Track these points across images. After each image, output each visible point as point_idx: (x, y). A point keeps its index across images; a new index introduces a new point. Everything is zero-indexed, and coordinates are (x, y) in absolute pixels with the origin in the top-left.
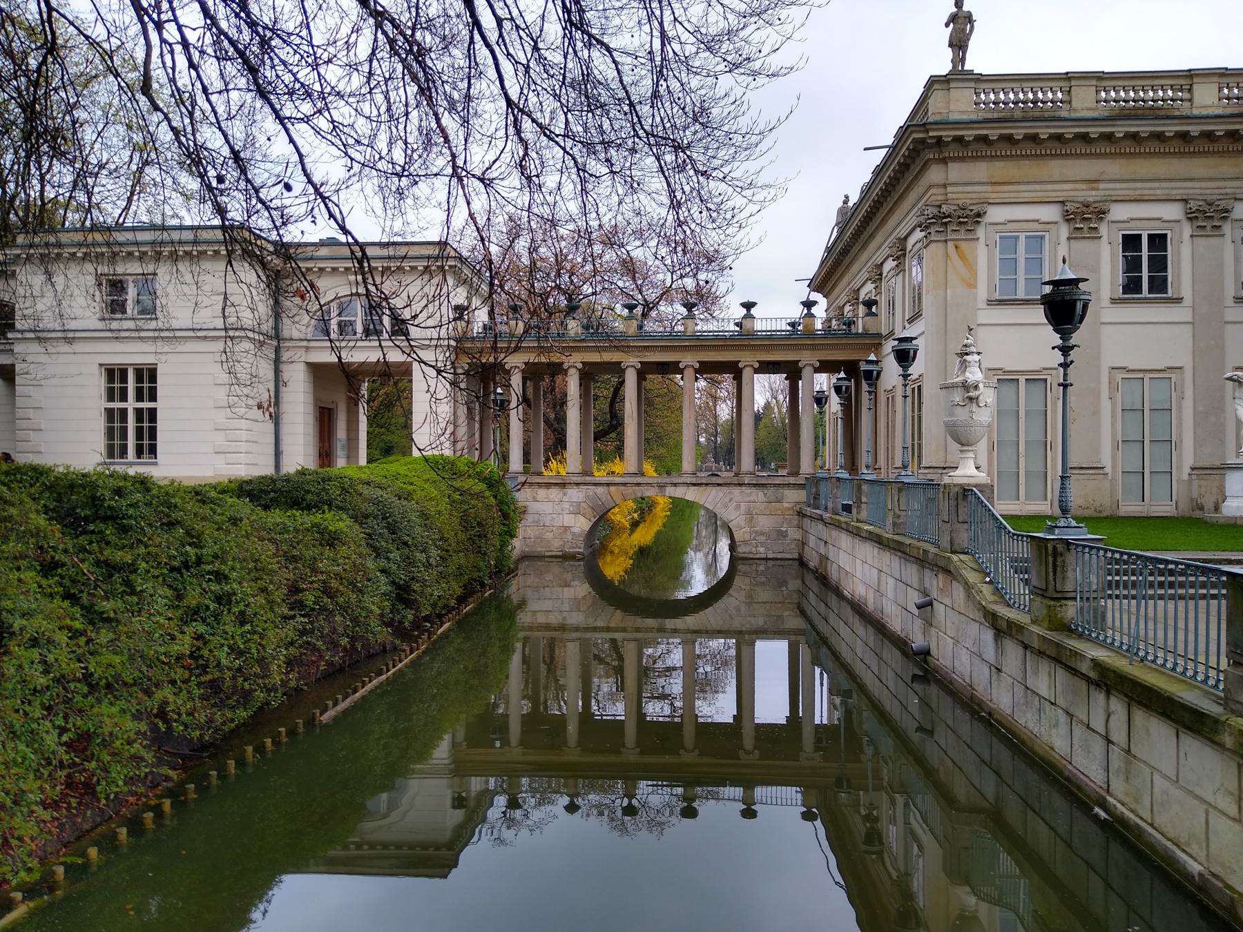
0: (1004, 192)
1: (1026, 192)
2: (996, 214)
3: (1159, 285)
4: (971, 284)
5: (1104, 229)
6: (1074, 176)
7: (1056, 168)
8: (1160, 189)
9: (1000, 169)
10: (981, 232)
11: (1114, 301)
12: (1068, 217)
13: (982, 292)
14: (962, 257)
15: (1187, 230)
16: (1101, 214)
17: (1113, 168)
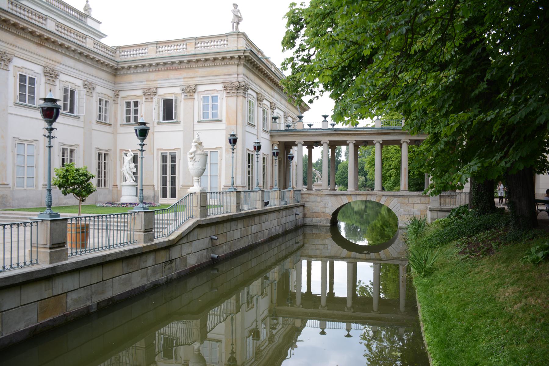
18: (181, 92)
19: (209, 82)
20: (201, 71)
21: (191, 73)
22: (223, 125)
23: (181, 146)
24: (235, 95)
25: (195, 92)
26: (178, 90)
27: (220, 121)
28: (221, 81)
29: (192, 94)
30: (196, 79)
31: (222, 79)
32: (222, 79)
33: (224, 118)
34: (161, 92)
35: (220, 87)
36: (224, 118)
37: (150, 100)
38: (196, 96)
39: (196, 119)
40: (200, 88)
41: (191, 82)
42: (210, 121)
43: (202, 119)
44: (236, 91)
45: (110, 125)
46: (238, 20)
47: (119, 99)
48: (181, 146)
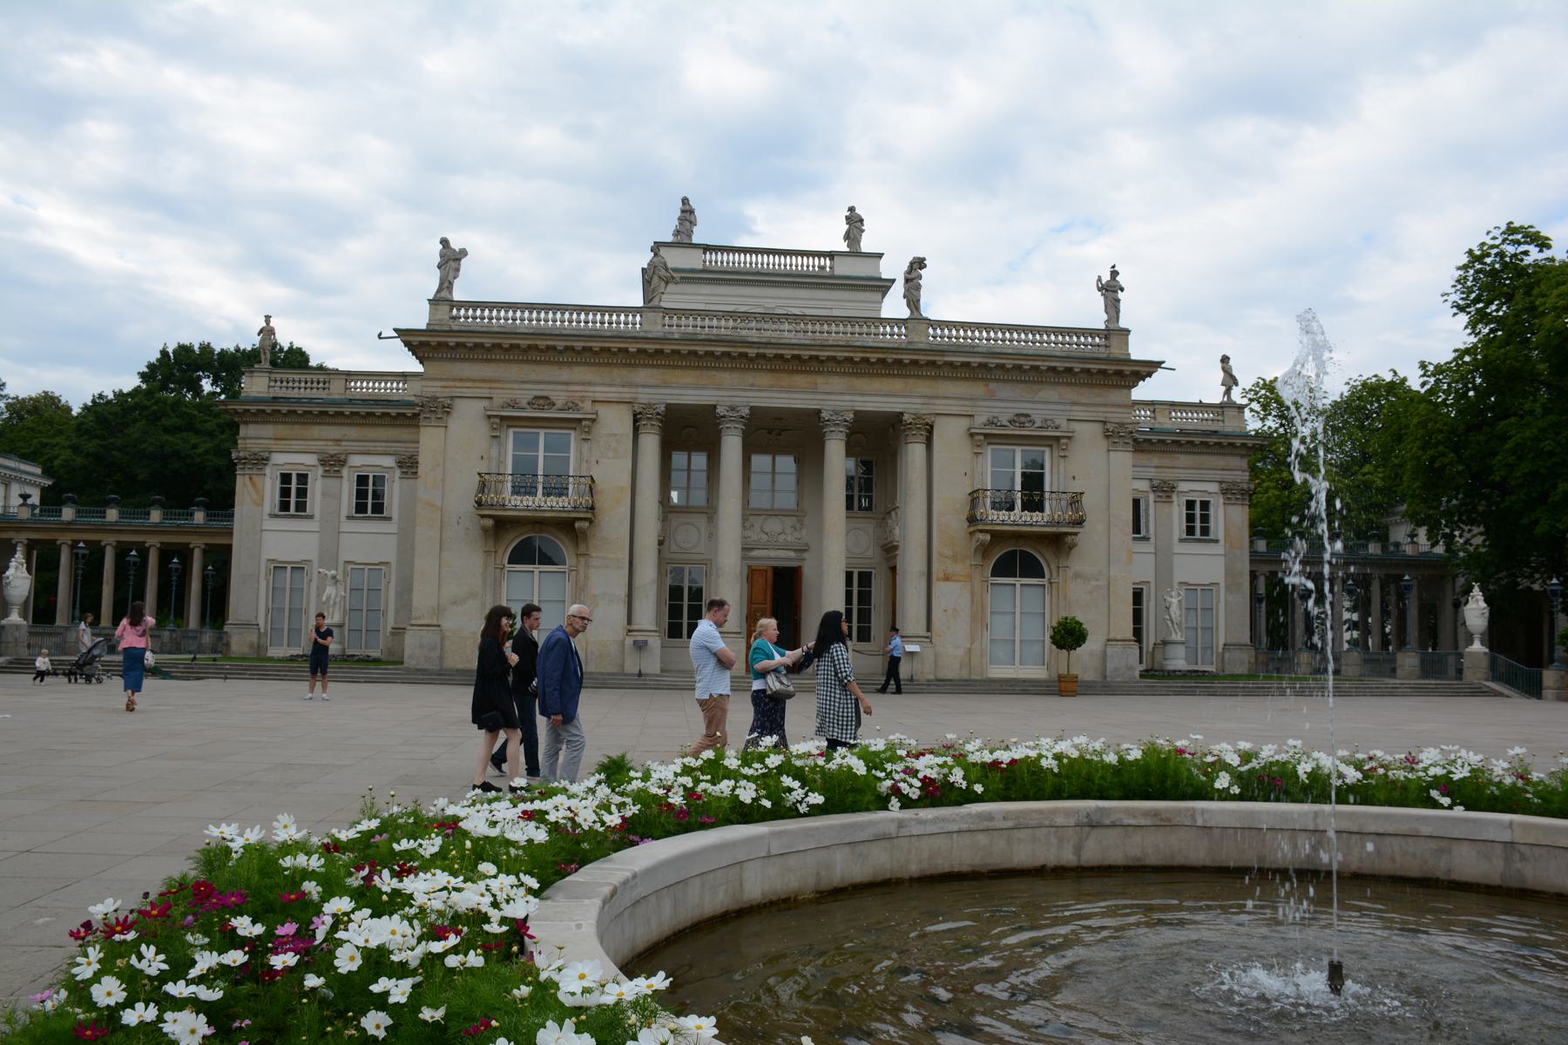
0: (282, 445)
1: (296, 445)
2: (278, 458)
3: (378, 508)
4: (261, 504)
5: (345, 472)
6: (326, 436)
7: (316, 431)
8: (381, 447)
9: (281, 430)
10: (268, 470)
11: (349, 518)
12: (323, 462)
13: (267, 508)
14: (253, 484)
15: (398, 473)
16: (343, 463)
17: (352, 432)
19: (1198, 477)
20: (1184, 459)
21: (1166, 460)
22: (1219, 549)
27: (1217, 541)
28: (1218, 478)
31: (1219, 475)
32: (1219, 475)
36: (1221, 536)
38: (1175, 497)
39: (1176, 537)
41: (1168, 475)
42: (1199, 541)
46: (1230, 381)
48: (1151, 579)
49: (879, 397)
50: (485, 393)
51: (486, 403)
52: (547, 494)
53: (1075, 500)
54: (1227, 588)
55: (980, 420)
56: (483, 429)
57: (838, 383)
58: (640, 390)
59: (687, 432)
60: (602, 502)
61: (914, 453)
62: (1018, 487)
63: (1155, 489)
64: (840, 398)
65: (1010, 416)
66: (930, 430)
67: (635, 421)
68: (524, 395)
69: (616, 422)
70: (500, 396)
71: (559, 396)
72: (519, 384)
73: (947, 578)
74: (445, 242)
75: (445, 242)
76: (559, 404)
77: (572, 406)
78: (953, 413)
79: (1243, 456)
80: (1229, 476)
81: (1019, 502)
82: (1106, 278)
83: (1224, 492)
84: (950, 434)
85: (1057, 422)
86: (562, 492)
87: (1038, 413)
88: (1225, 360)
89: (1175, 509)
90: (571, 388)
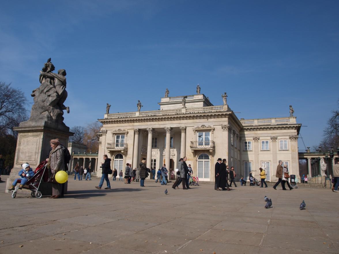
18: (270, 139)
23: (254, 160)
24: (295, 140)
25: (277, 139)
26: (269, 138)
29: (275, 140)
30: (277, 134)
33: (290, 150)
34: (261, 138)
35: (288, 137)
36: (290, 150)
37: (256, 141)
38: (277, 140)
40: (279, 138)
42: (284, 150)
43: (280, 149)
44: (295, 139)
45: (251, 151)
47: (242, 141)
48: (272, 160)
49: (175, 124)
50: (112, 129)
51: (112, 131)
52: (120, 146)
53: (214, 143)
54: (292, 162)
55: (196, 127)
56: (193, 133)
57: (167, 122)
58: (135, 127)
59: (142, 133)
60: (129, 147)
61: (183, 135)
62: (204, 140)
63: (271, 139)
64: (168, 125)
65: (201, 126)
66: (185, 129)
67: (134, 132)
68: (117, 129)
69: (131, 133)
70: (114, 130)
71: (122, 129)
72: (116, 127)
73: (188, 160)
74: (108, 104)
75: (108, 104)
76: (122, 131)
77: (124, 130)
78: (190, 125)
79: (295, 129)
80: (291, 134)
81: (204, 143)
82: (224, 95)
83: (290, 138)
84: (190, 131)
85: (211, 126)
86: (208, 144)
87: (207, 125)
88: (291, 106)
89: (277, 143)
90: (124, 127)
